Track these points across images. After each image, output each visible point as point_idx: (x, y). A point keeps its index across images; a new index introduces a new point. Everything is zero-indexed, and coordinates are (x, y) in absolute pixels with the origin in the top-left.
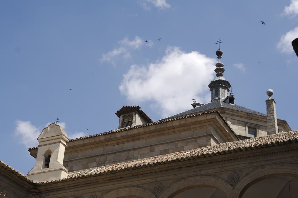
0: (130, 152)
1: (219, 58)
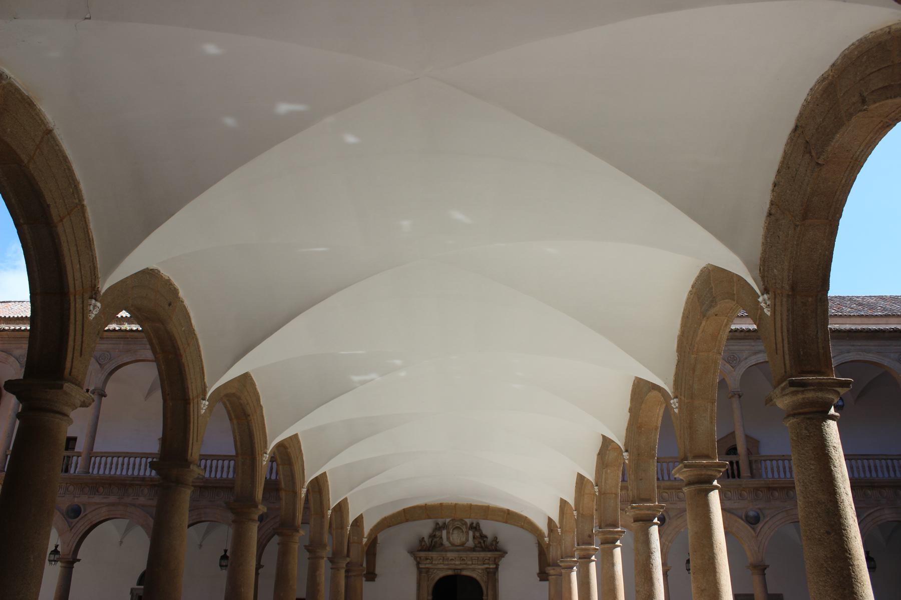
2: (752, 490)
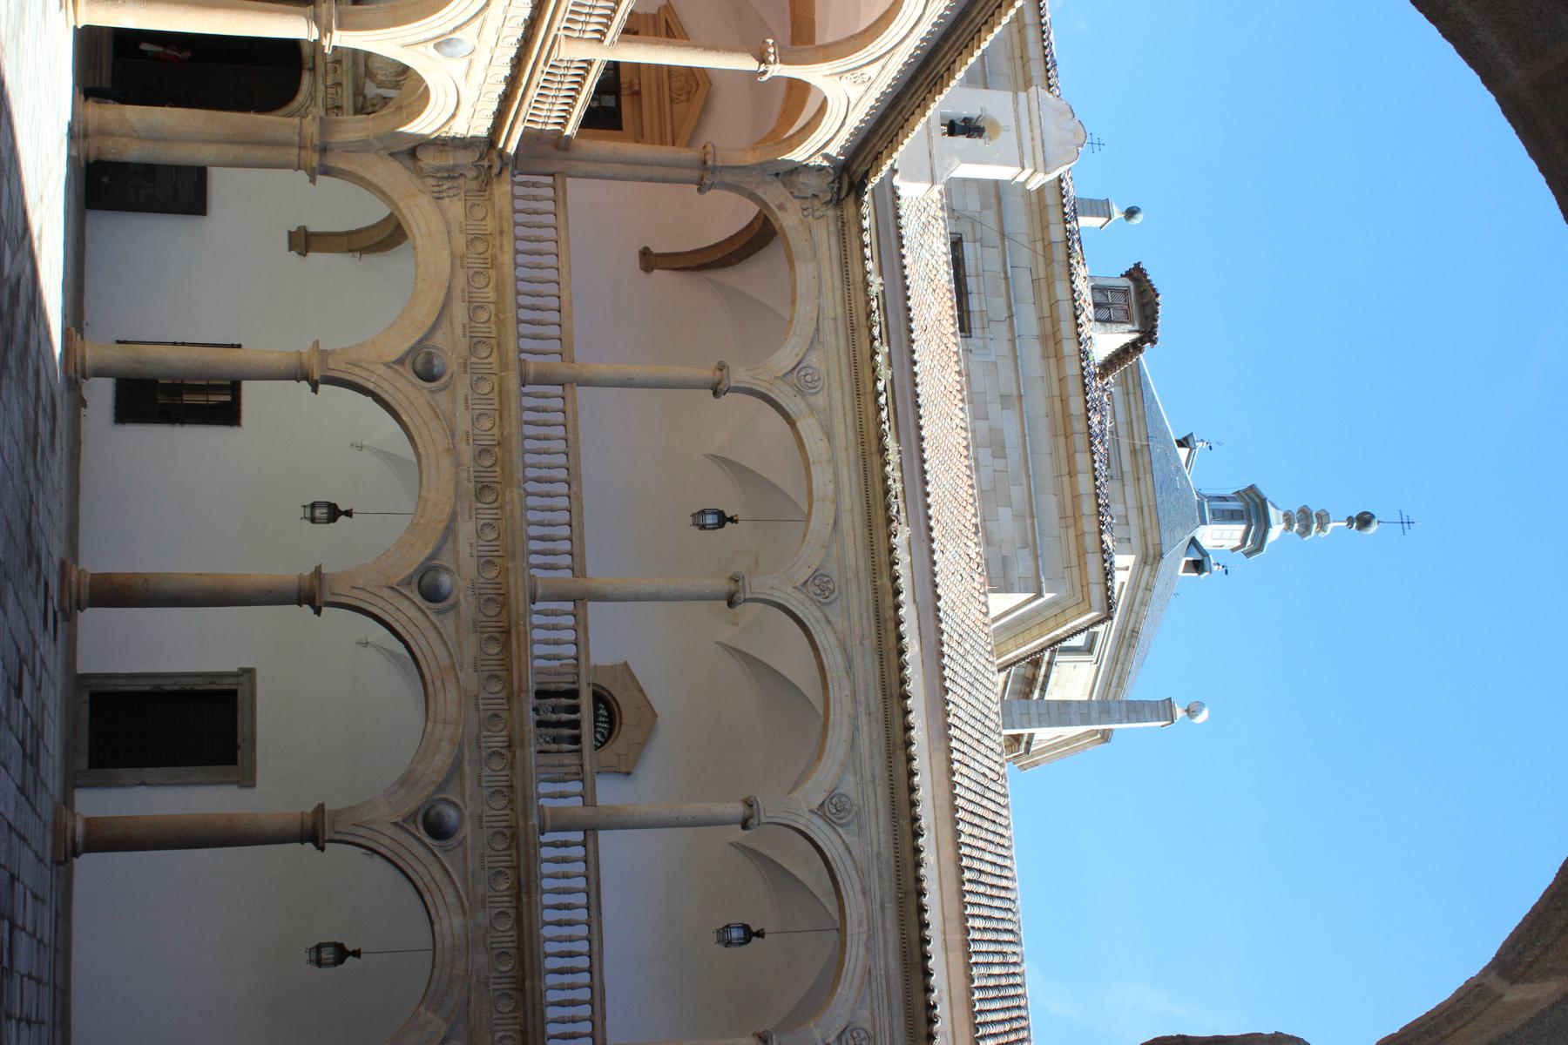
0: (1004, 327)
1: (1350, 520)
2: (501, 592)
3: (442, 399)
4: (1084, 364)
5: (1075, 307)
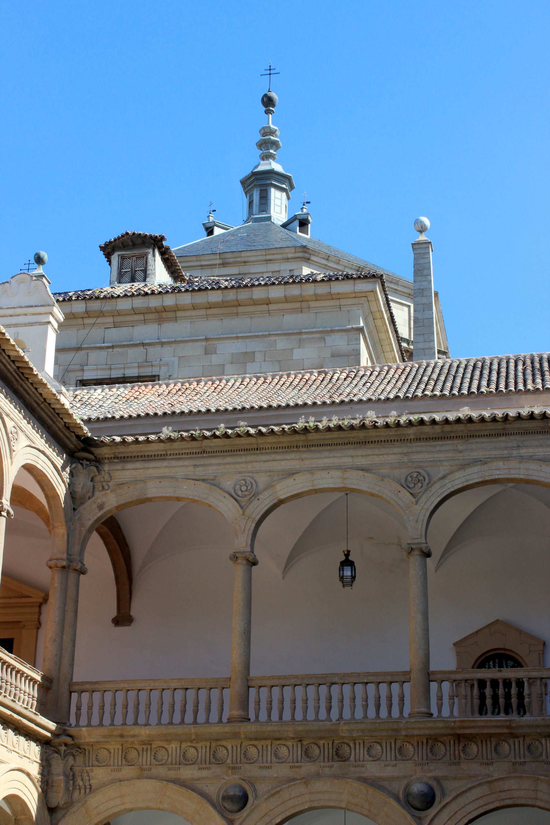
0: (151, 350)
1: (268, 112)
2: (425, 741)
3: (262, 788)
4: (183, 290)
5: (138, 295)
